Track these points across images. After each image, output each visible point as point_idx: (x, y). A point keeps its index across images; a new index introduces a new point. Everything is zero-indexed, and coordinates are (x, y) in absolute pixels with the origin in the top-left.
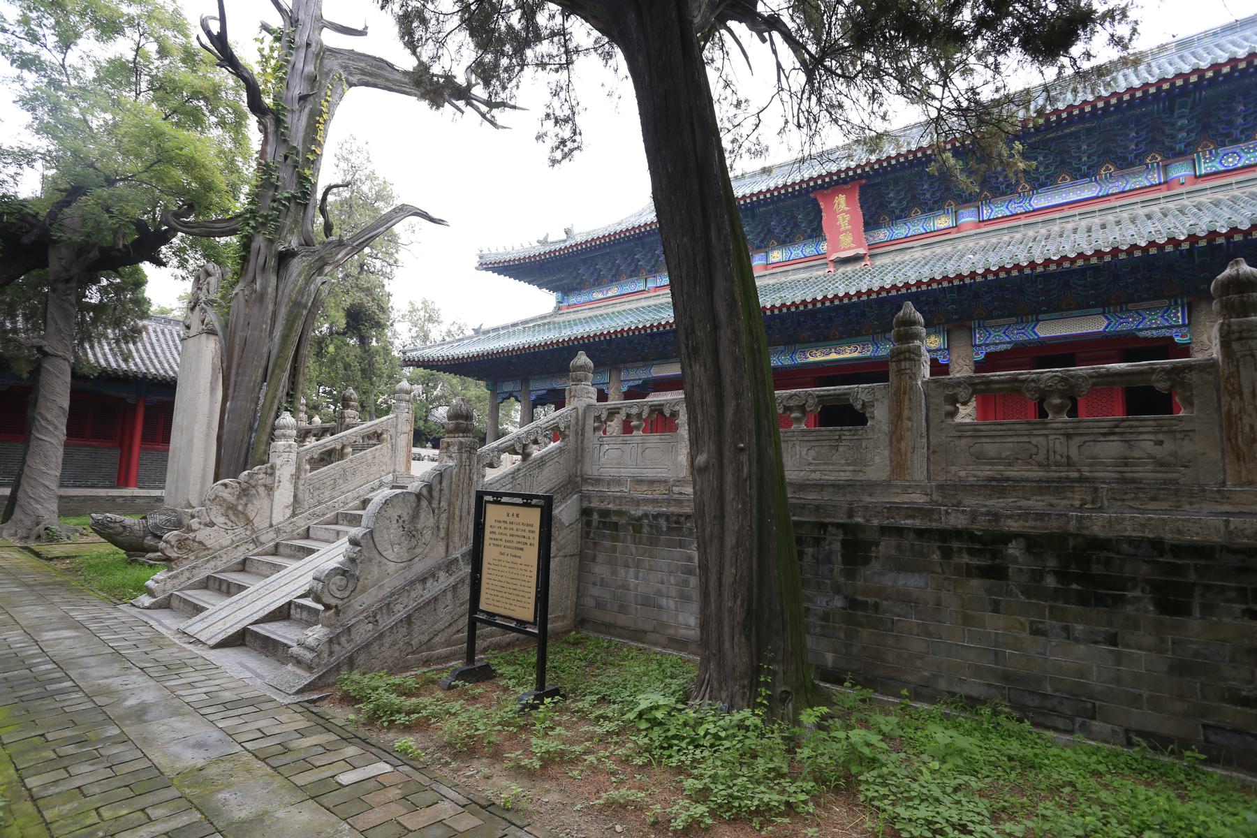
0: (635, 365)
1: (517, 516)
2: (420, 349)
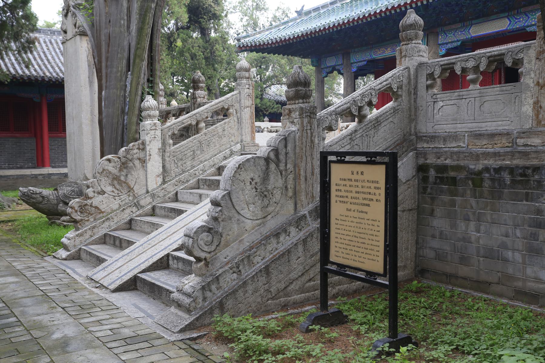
0: (453, 26)
1: (362, 173)
2: (252, 35)
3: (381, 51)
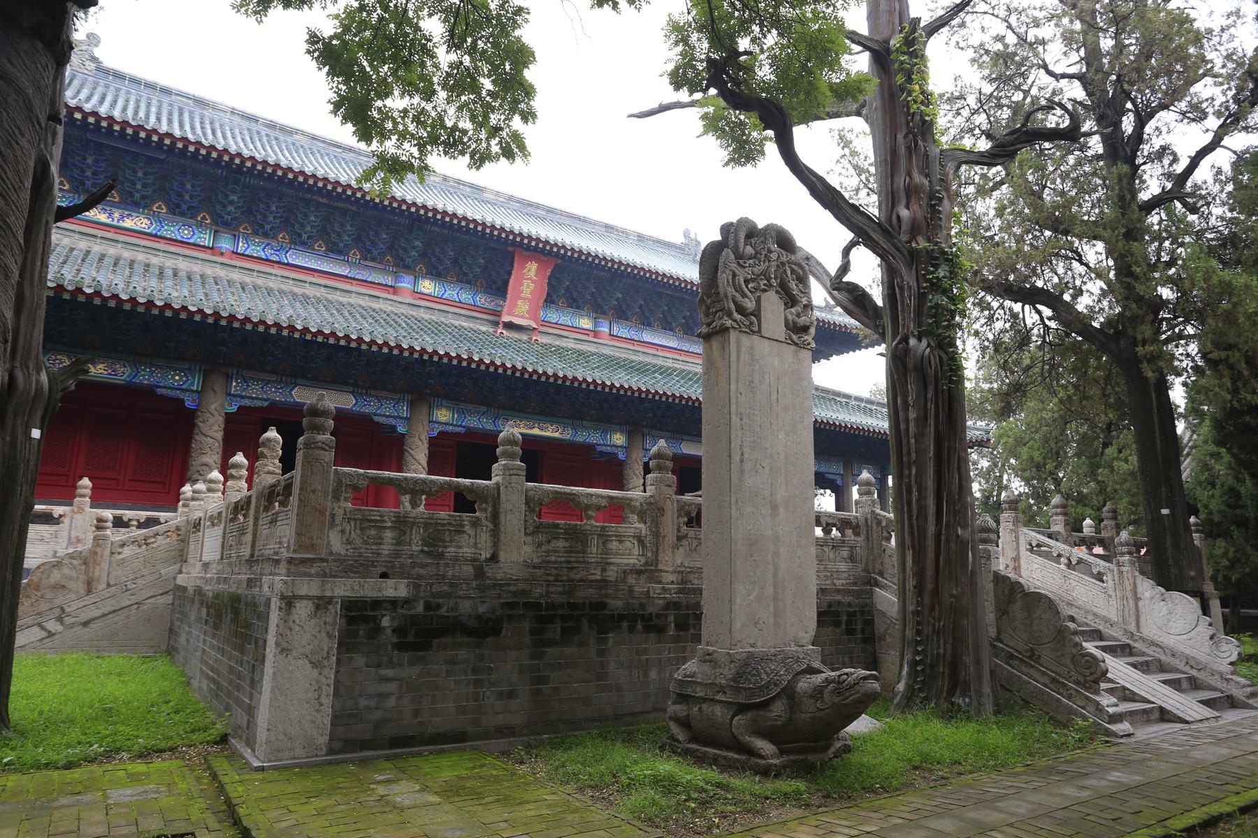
0: (262, 376)
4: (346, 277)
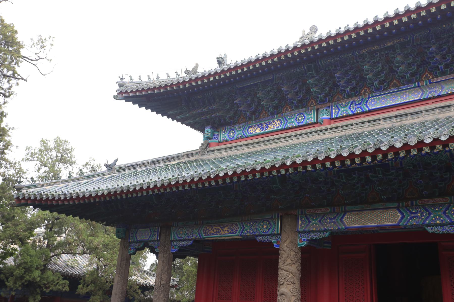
0: (319, 211)
2: (39, 186)
3: (215, 230)
4: (421, 100)
